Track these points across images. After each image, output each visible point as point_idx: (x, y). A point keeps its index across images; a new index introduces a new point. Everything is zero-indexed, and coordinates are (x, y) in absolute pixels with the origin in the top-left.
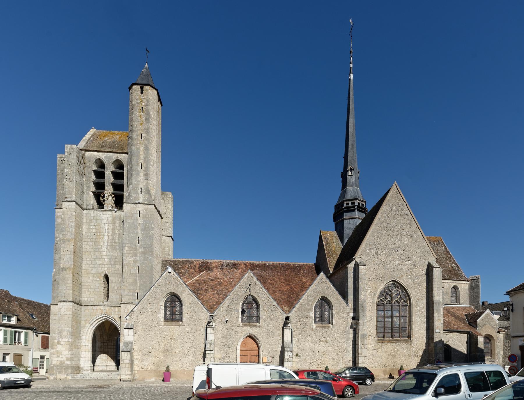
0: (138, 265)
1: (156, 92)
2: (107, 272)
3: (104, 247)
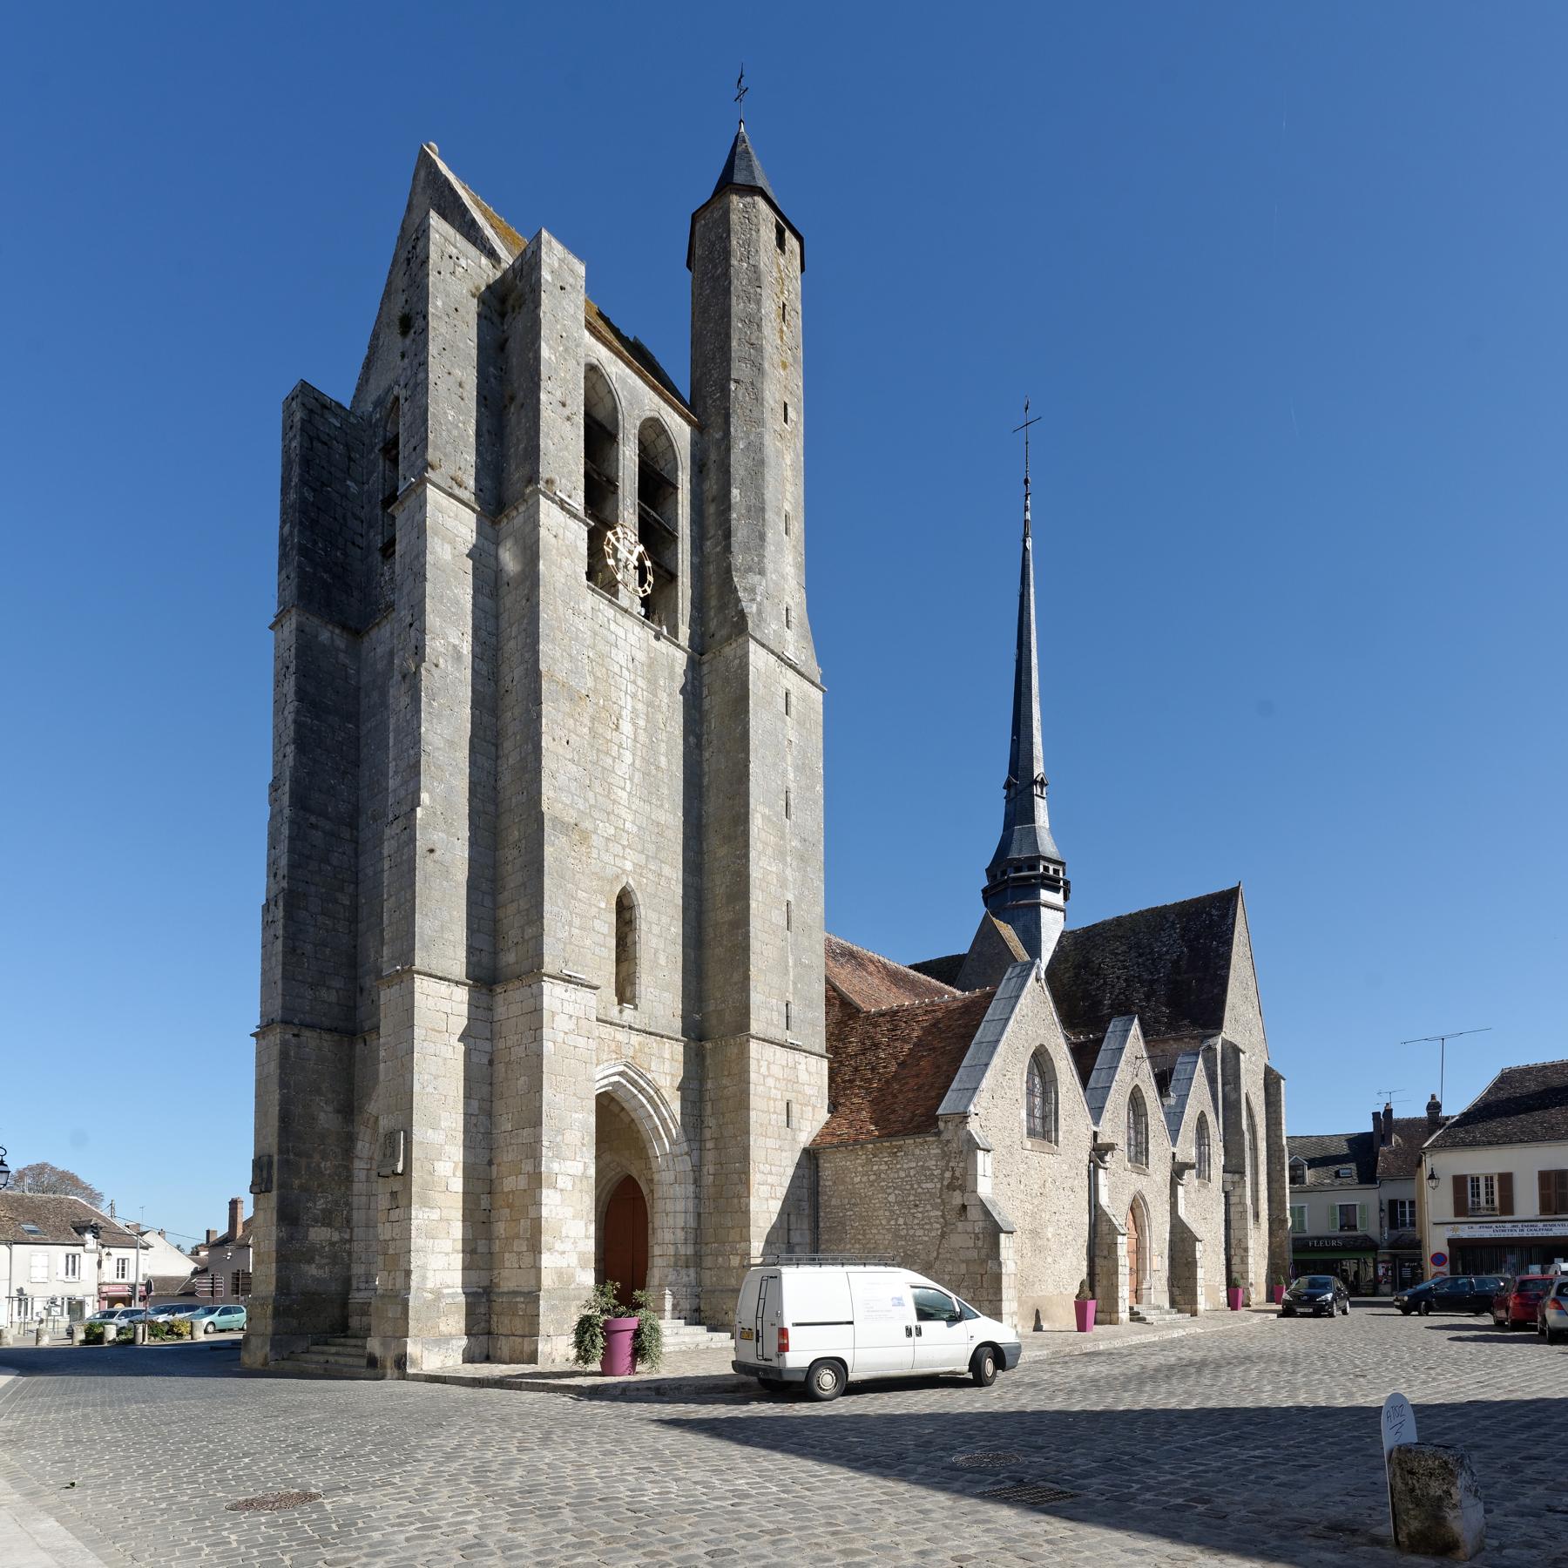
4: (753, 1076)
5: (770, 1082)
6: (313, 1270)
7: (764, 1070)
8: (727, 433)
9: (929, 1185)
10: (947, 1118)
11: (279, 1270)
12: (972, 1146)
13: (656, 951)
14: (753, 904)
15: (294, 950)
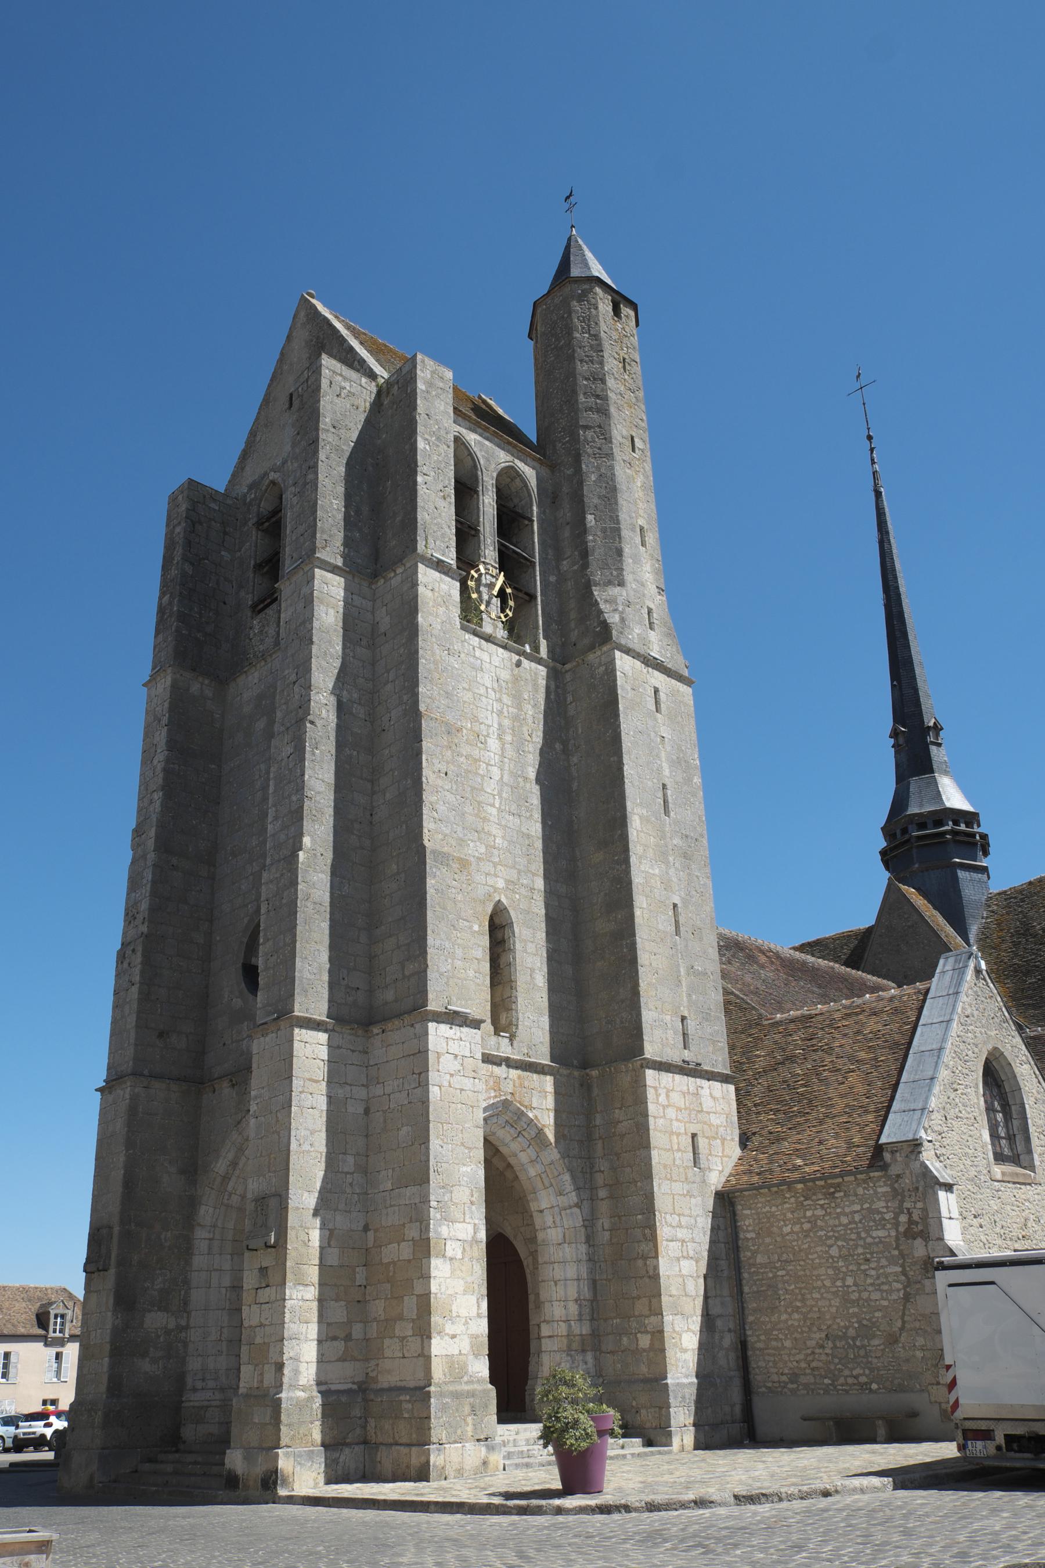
0: (676, 900)
2: (504, 900)
3: (491, 787)
4: (652, 1108)
5: (671, 1113)
6: (146, 1366)
7: (662, 1099)
8: (578, 470)
9: (881, 1233)
10: (895, 1147)
11: (112, 1366)
12: (930, 1185)
13: (532, 970)
14: (638, 913)
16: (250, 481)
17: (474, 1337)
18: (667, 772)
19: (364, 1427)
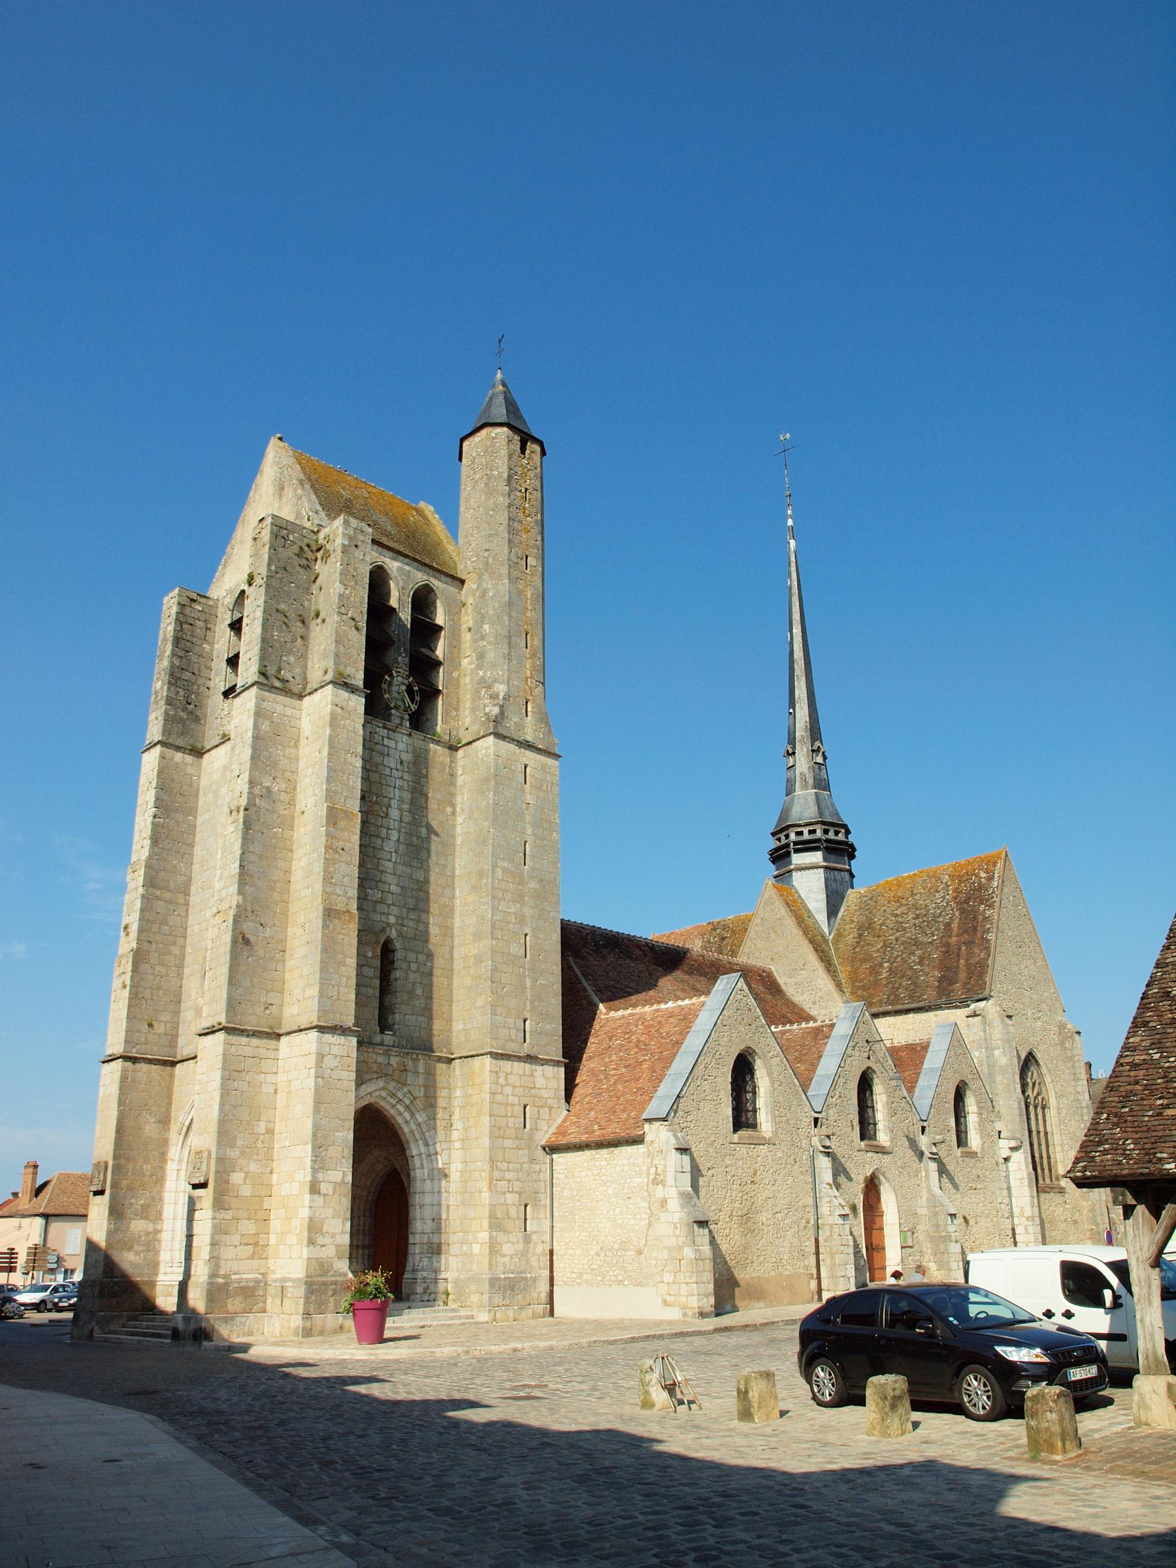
0: (528, 930)
1: (466, 444)
2: (394, 934)
9: (640, 1180)
13: (414, 984)
15: (136, 994)
16: (227, 587)
17: (338, 1246)
18: (529, 831)
19: (265, 1302)
